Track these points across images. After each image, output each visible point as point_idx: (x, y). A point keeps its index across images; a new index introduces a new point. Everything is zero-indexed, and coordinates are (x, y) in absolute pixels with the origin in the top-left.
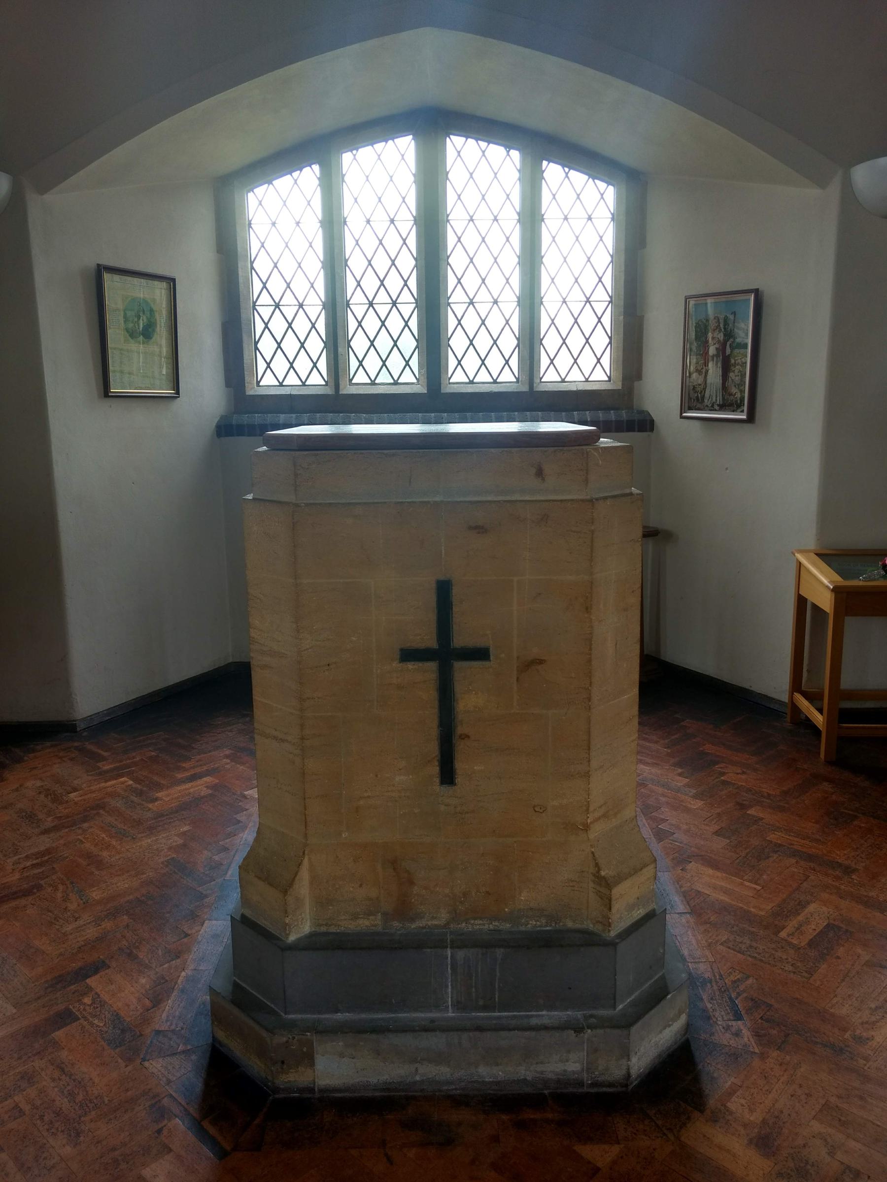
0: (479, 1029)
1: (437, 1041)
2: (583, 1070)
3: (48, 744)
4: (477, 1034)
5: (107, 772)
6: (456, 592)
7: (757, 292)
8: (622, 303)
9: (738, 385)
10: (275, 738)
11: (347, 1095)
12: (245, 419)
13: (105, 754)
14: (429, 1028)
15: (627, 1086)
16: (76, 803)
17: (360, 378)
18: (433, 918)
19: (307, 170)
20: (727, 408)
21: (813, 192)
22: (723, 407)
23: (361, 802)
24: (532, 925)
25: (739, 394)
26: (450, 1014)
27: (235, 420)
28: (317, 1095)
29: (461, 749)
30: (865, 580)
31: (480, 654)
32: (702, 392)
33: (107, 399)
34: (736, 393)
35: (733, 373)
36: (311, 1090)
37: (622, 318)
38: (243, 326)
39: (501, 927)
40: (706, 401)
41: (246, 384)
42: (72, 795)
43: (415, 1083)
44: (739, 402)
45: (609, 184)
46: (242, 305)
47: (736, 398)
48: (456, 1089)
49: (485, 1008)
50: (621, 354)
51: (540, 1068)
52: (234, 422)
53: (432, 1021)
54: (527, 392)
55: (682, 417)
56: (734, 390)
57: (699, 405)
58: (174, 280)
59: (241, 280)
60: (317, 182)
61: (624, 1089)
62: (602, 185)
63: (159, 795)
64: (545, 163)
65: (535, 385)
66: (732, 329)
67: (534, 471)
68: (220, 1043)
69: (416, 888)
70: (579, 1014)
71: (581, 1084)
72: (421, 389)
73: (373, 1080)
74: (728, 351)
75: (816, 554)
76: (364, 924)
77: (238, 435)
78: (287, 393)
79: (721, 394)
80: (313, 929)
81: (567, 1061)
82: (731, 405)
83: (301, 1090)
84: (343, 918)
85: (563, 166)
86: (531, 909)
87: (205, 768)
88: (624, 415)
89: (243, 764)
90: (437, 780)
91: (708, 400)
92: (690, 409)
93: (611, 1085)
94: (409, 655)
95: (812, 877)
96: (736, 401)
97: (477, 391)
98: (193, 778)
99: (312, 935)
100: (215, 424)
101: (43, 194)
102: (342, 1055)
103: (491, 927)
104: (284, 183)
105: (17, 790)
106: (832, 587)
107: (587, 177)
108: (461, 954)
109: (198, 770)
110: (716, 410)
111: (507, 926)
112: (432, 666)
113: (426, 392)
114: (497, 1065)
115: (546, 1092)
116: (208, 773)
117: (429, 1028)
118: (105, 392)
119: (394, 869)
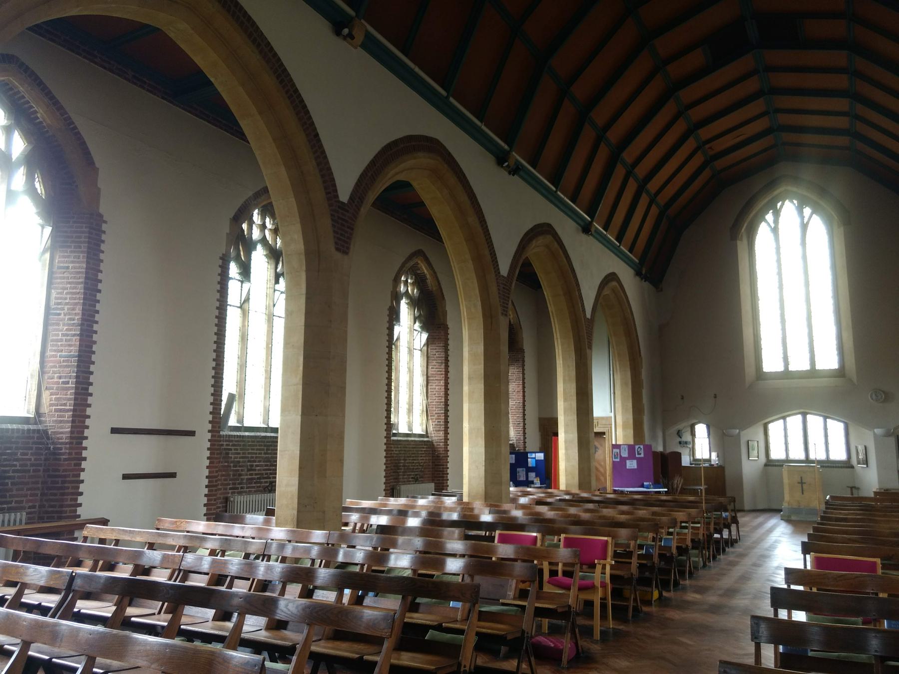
6: (803, 478)
12: (770, 463)
27: (768, 464)
31: (805, 483)
58: (758, 441)
88: (847, 465)
94: (798, 483)
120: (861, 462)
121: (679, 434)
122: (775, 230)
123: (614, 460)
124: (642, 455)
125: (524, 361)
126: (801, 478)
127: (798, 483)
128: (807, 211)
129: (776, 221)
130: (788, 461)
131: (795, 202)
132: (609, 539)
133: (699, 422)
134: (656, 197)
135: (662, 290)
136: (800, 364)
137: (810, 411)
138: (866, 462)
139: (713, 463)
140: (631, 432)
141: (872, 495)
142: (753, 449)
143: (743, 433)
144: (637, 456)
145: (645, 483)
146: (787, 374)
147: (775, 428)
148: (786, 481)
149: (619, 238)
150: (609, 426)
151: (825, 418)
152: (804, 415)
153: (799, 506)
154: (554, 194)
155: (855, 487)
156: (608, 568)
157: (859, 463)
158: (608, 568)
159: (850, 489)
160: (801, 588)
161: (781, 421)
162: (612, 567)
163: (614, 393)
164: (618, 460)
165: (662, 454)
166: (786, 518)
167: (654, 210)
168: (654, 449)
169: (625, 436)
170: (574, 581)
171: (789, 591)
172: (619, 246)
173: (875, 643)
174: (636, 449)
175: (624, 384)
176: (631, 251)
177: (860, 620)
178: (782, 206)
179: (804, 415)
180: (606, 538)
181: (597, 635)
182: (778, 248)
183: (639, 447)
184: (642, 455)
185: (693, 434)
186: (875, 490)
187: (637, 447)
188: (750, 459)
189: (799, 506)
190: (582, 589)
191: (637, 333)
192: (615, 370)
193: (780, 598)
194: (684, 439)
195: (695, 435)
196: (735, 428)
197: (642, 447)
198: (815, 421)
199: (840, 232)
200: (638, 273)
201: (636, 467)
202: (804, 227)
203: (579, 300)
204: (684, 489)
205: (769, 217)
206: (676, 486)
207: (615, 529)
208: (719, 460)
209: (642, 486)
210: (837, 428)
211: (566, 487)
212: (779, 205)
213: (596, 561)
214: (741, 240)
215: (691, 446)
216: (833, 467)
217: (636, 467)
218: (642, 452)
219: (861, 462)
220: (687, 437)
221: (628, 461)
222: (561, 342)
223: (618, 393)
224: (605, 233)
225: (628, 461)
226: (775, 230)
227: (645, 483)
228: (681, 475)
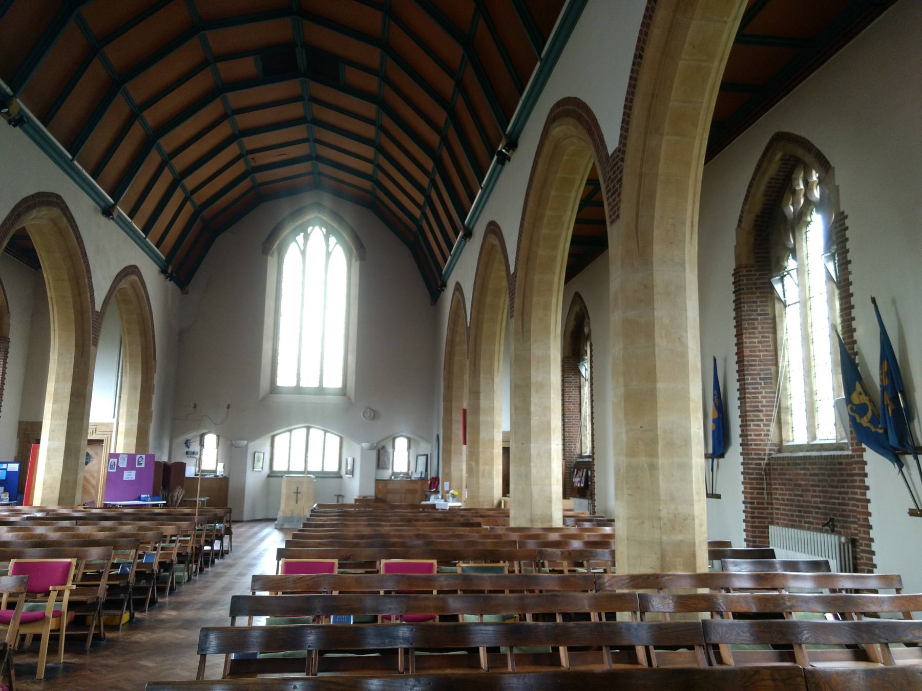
12: (272, 475)
120: (349, 472)
121: (187, 444)
122: (303, 253)
123: (109, 470)
124: (143, 466)
125: (7, 352)
126: (297, 488)
127: (295, 493)
128: (333, 240)
129: (305, 244)
130: (289, 472)
131: (324, 230)
132: (74, 561)
133: (210, 432)
134: (192, 195)
135: (187, 293)
136: (310, 381)
137: (293, 427)
138: (352, 473)
139: (218, 474)
140: (133, 440)
141: (353, 502)
142: (259, 461)
143: (251, 444)
144: (137, 466)
145: (142, 496)
146: (298, 390)
147: (282, 440)
148: (284, 491)
149: (146, 229)
150: (110, 433)
151: (326, 432)
152: (308, 428)
153: (292, 514)
154: (69, 163)
155: (340, 495)
156: (67, 595)
157: (347, 474)
158: (67, 595)
159: (336, 497)
160: (267, 594)
161: (288, 433)
162: (72, 593)
163: (120, 397)
164: (115, 471)
165: (165, 464)
166: (279, 527)
167: (188, 209)
168: (157, 459)
169: (126, 445)
170: (16, 614)
171: (254, 598)
172: (145, 239)
173: (311, 638)
174: (137, 459)
175: (132, 388)
176: (158, 245)
177: (311, 617)
178: (311, 232)
179: (308, 428)
180: (69, 560)
181: (41, 673)
182: (304, 270)
183: (141, 457)
184: (143, 466)
185: (202, 445)
186: (355, 498)
187: (138, 456)
189: (292, 514)
190: (25, 622)
191: (153, 332)
192: (124, 372)
193: (240, 606)
194: (191, 449)
195: (203, 446)
196: (245, 440)
197: (144, 456)
198: (316, 434)
199: (356, 265)
200: (163, 271)
201: (134, 478)
202: (328, 254)
203: (88, 289)
204: (185, 501)
205: (300, 238)
206: (176, 498)
207: (83, 548)
208: (224, 471)
209: (139, 499)
210: (333, 440)
211: (42, 503)
212: (310, 229)
213: (51, 588)
214: (272, 256)
215: (198, 456)
216: (324, 477)
217: (134, 478)
218: (143, 462)
219: (349, 472)
220: (195, 447)
221: (125, 472)
222: (59, 334)
223: (124, 397)
224: (130, 221)
225: (125, 472)
226: (303, 253)
227: (142, 496)
228: (182, 487)
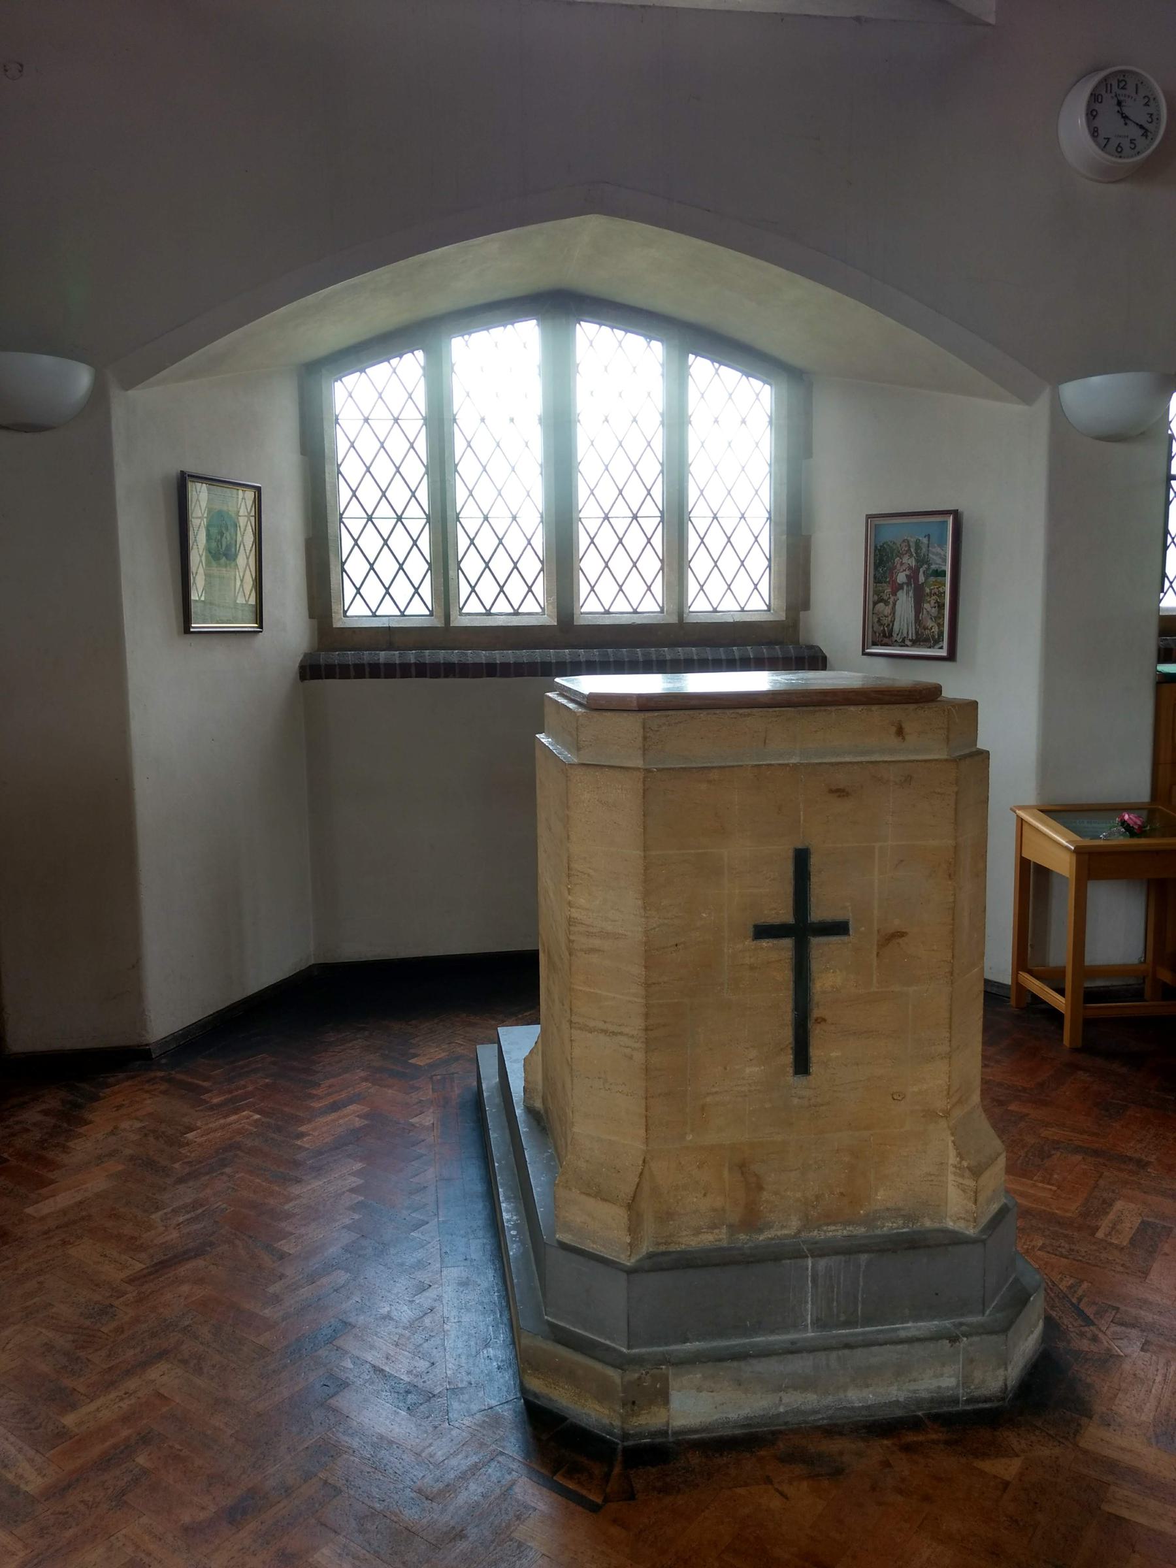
0: (848, 1346)
1: (801, 1365)
2: (958, 1385)
3: (121, 1076)
4: (846, 1352)
5: (219, 1105)
6: (814, 861)
7: (956, 514)
8: (784, 520)
9: (935, 617)
10: (605, 1032)
11: (704, 1435)
12: (336, 657)
13: (206, 1084)
14: (793, 1350)
15: (1003, 1399)
16: (200, 1145)
17: (473, 607)
18: (783, 1227)
19: (408, 357)
20: (922, 644)
21: (1019, 408)
22: (915, 643)
23: (708, 1099)
24: (889, 1227)
25: (937, 627)
26: (810, 1334)
27: (324, 658)
28: (671, 1439)
29: (817, 1034)
30: (1106, 837)
31: (839, 928)
32: (889, 625)
33: (188, 636)
34: (932, 626)
35: (928, 604)
36: (664, 1433)
37: (784, 537)
38: (331, 544)
39: (855, 1233)
40: (895, 635)
41: (333, 614)
42: (190, 1136)
43: (779, 1415)
44: (937, 637)
45: (765, 382)
46: (330, 518)
47: (933, 632)
48: (823, 1419)
49: (848, 1324)
50: (784, 579)
51: (913, 1386)
52: (322, 662)
53: (793, 1343)
54: (676, 623)
55: (864, 654)
56: (930, 624)
57: (886, 640)
58: (258, 489)
59: (328, 488)
60: (421, 372)
61: (1001, 1403)
62: (756, 384)
63: (303, 1129)
64: (691, 357)
65: (685, 615)
66: (926, 554)
67: (893, 729)
68: (536, 1395)
69: (765, 1193)
70: (947, 1323)
71: (955, 1401)
72: (550, 620)
73: (733, 1416)
74: (922, 579)
75: (1042, 811)
76: (708, 1239)
77: (327, 678)
78: (385, 626)
79: (914, 627)
80: (651, 1249)
81: (942, 1375)
82: (927, 640)
83: (653, 1435)
84: (685, 1233)
85: (713, 361)
86: (888, 1209)
87: (344, 1095)
88: (792, 651)
89: (389, 1087)
90: (791, 1070)
91: (898, 635)
92: (874, 644)
93: (987, 1400)
94: (763, 932)
95: (1106, 1173)
96: (933, 636)
97: (617, 622)
98: (335, 1107)
99: (651, 1256)
100: (298, 665)
101: (127, 390)
102: (699, 1389)
103: (845, 1233)
104: (379, 372)
105: (112, 1133)
106: (1073, 848)
107: (740, 374)
108: (822, 1263)
109: (336, 1097)
110: (907, 646)
111: (862, 1230)
112: (788, 943)
113: (556, 624)
114: (867, 1386)
115: (920, 1413)
116: (350, 1101)
117: (793, 1350)
118: (187, 630)
119: (742, 1173)
142: (222, 553)
153: (751, 1220)
188: (196, 626)
